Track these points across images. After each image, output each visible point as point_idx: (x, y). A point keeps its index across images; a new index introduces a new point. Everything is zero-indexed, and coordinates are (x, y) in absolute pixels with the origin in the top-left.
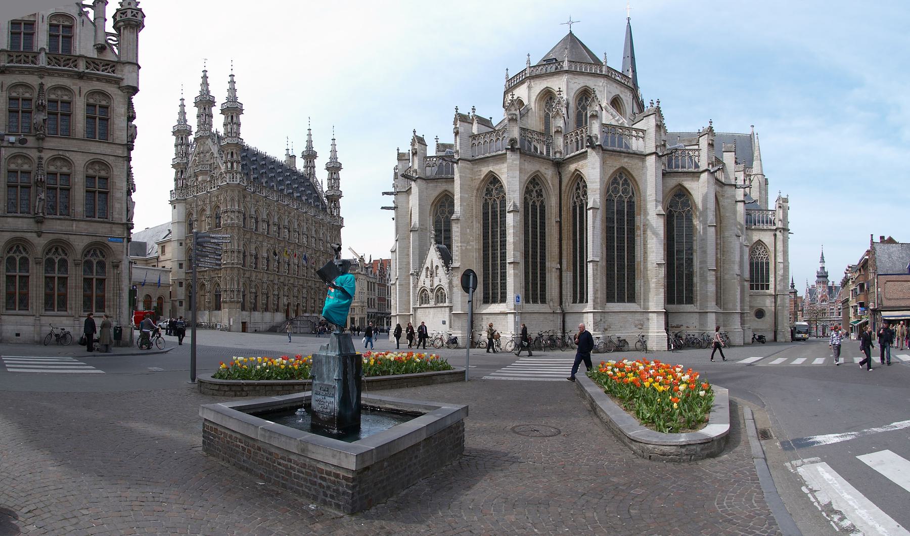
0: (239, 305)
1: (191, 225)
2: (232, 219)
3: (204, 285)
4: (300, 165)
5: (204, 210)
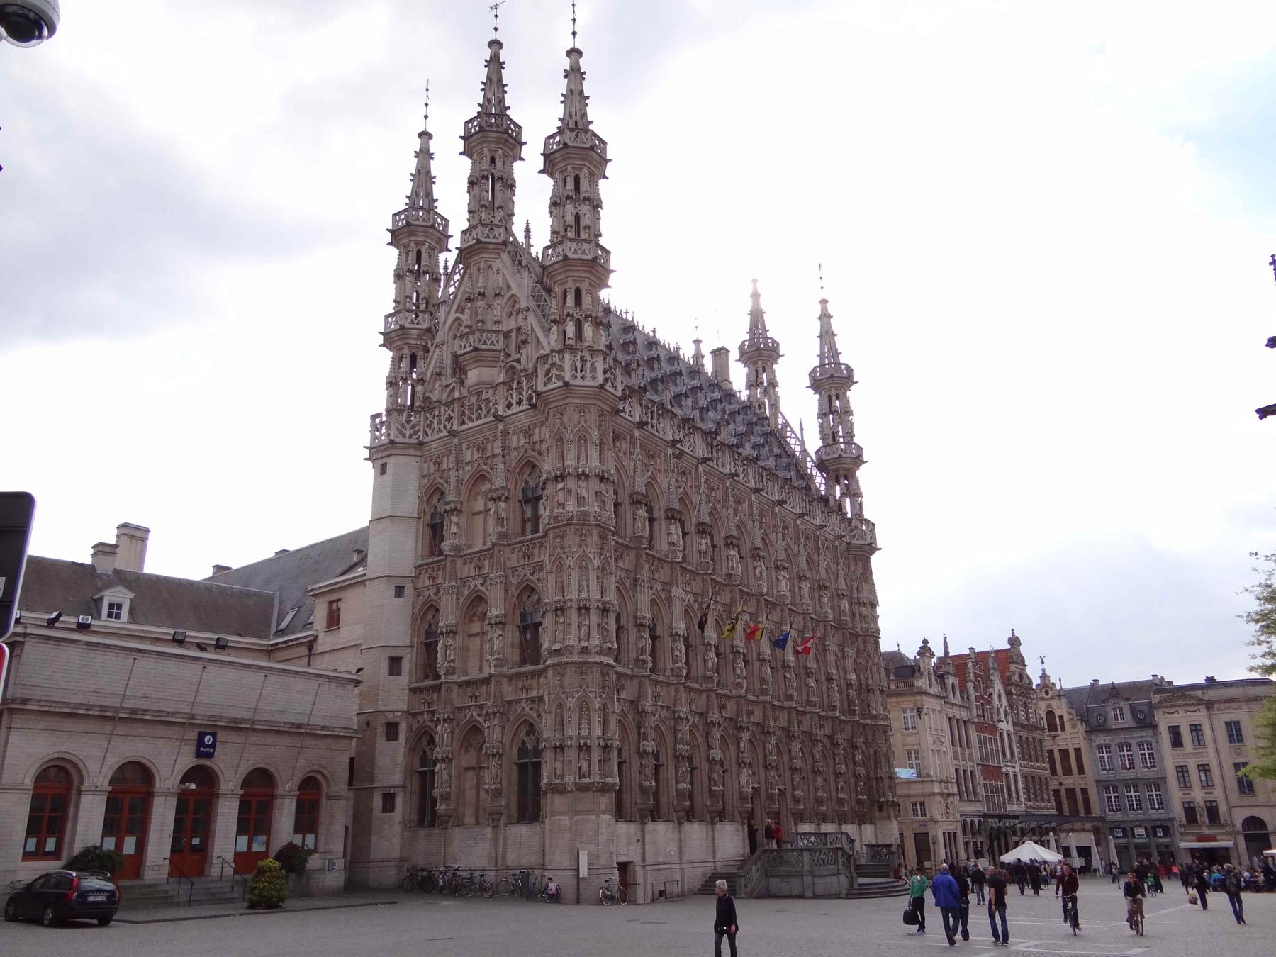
0: (606, 801)
1: (436, 530)
2: (580, 501)
3: (476, 729)
4: (738, 377)
5: (481, 477)
